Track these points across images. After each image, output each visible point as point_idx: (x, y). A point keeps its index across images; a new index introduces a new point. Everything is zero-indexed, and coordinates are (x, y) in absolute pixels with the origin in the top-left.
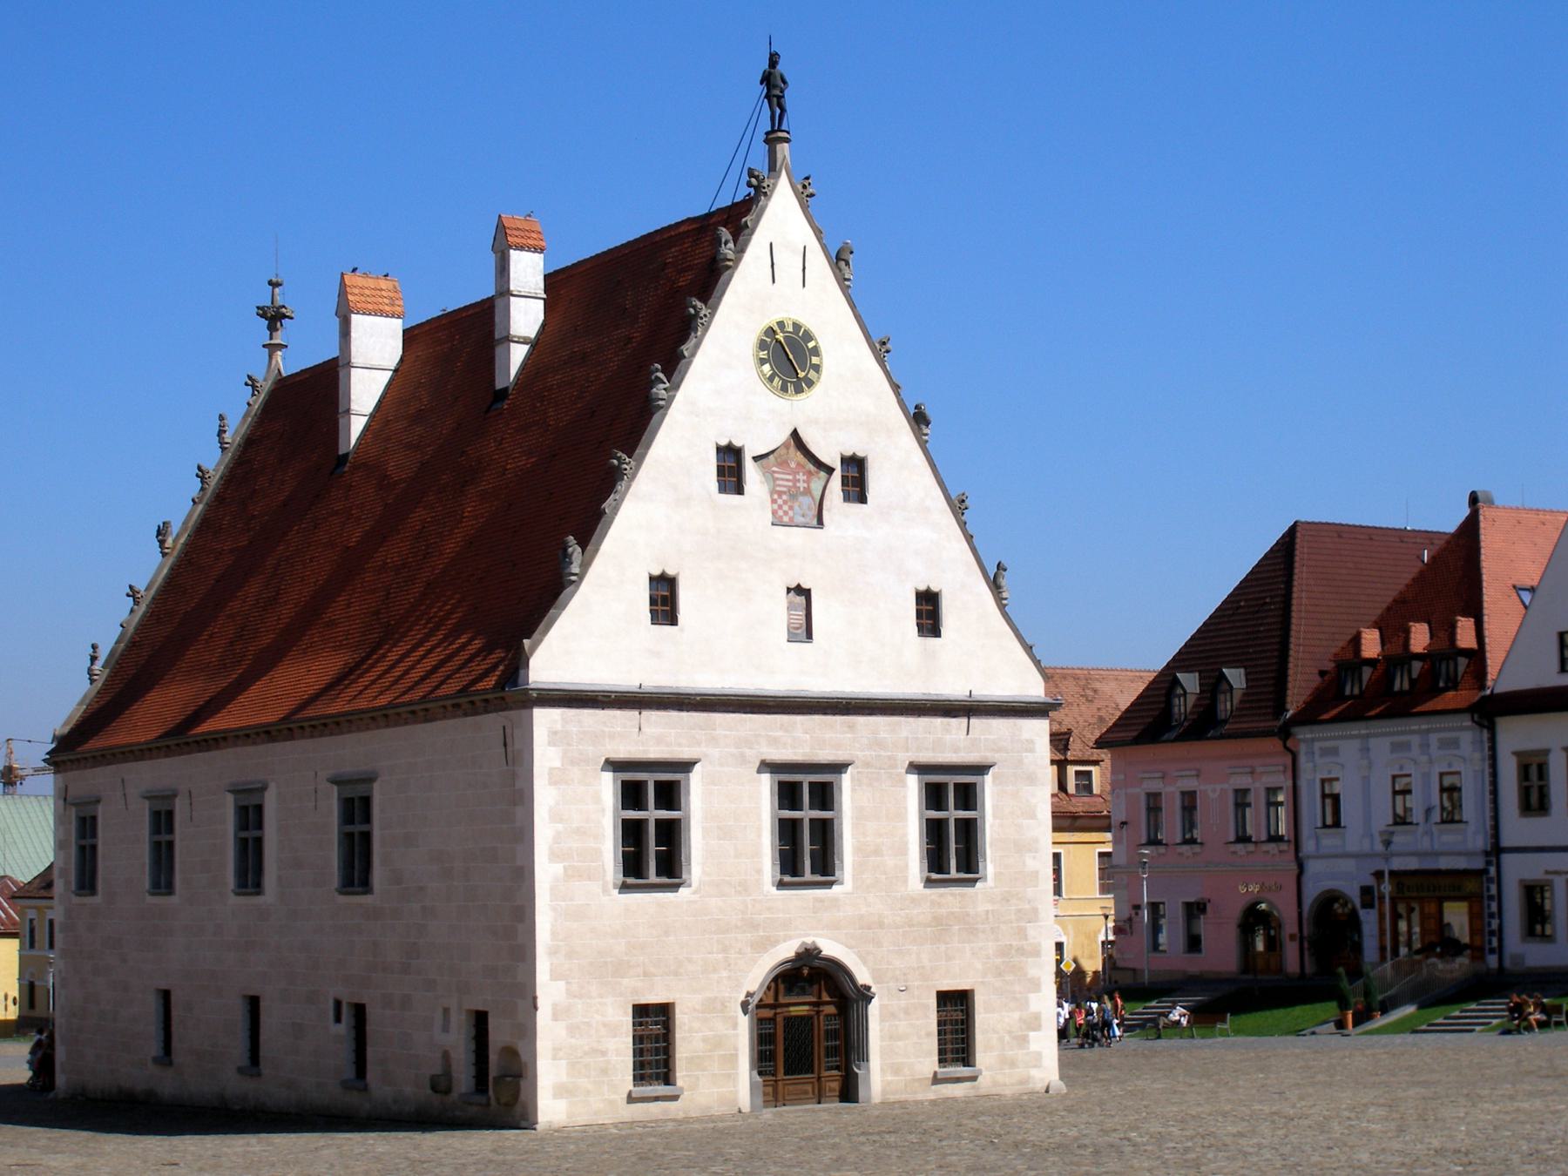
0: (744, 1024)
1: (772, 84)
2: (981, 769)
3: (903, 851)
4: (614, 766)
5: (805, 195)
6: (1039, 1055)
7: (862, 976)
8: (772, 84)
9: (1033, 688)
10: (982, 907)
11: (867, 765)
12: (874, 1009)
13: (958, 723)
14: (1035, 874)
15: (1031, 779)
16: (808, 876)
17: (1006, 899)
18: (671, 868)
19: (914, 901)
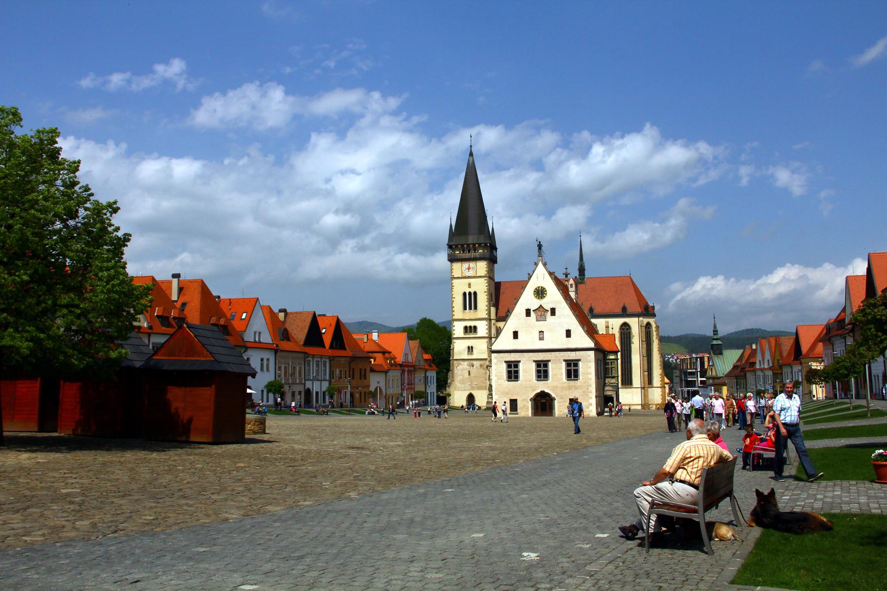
0: (530, 402)
1: (540, 246)
2: (579, 360)
3: (562, 374)
4: (506, 362)
5: (545, 265)
6: (591, 410)
7: (553, 395)
8: (540, 246)
9: (591, 345)
10: (579, 384)
11: (554, 360)
12: (556, 402)
13: (573, 353)
14: (591, 379)
15: (590, 362)
16: (513, 379)
17: (585, 383)
18: (516, 378)
19: (564, 383)
